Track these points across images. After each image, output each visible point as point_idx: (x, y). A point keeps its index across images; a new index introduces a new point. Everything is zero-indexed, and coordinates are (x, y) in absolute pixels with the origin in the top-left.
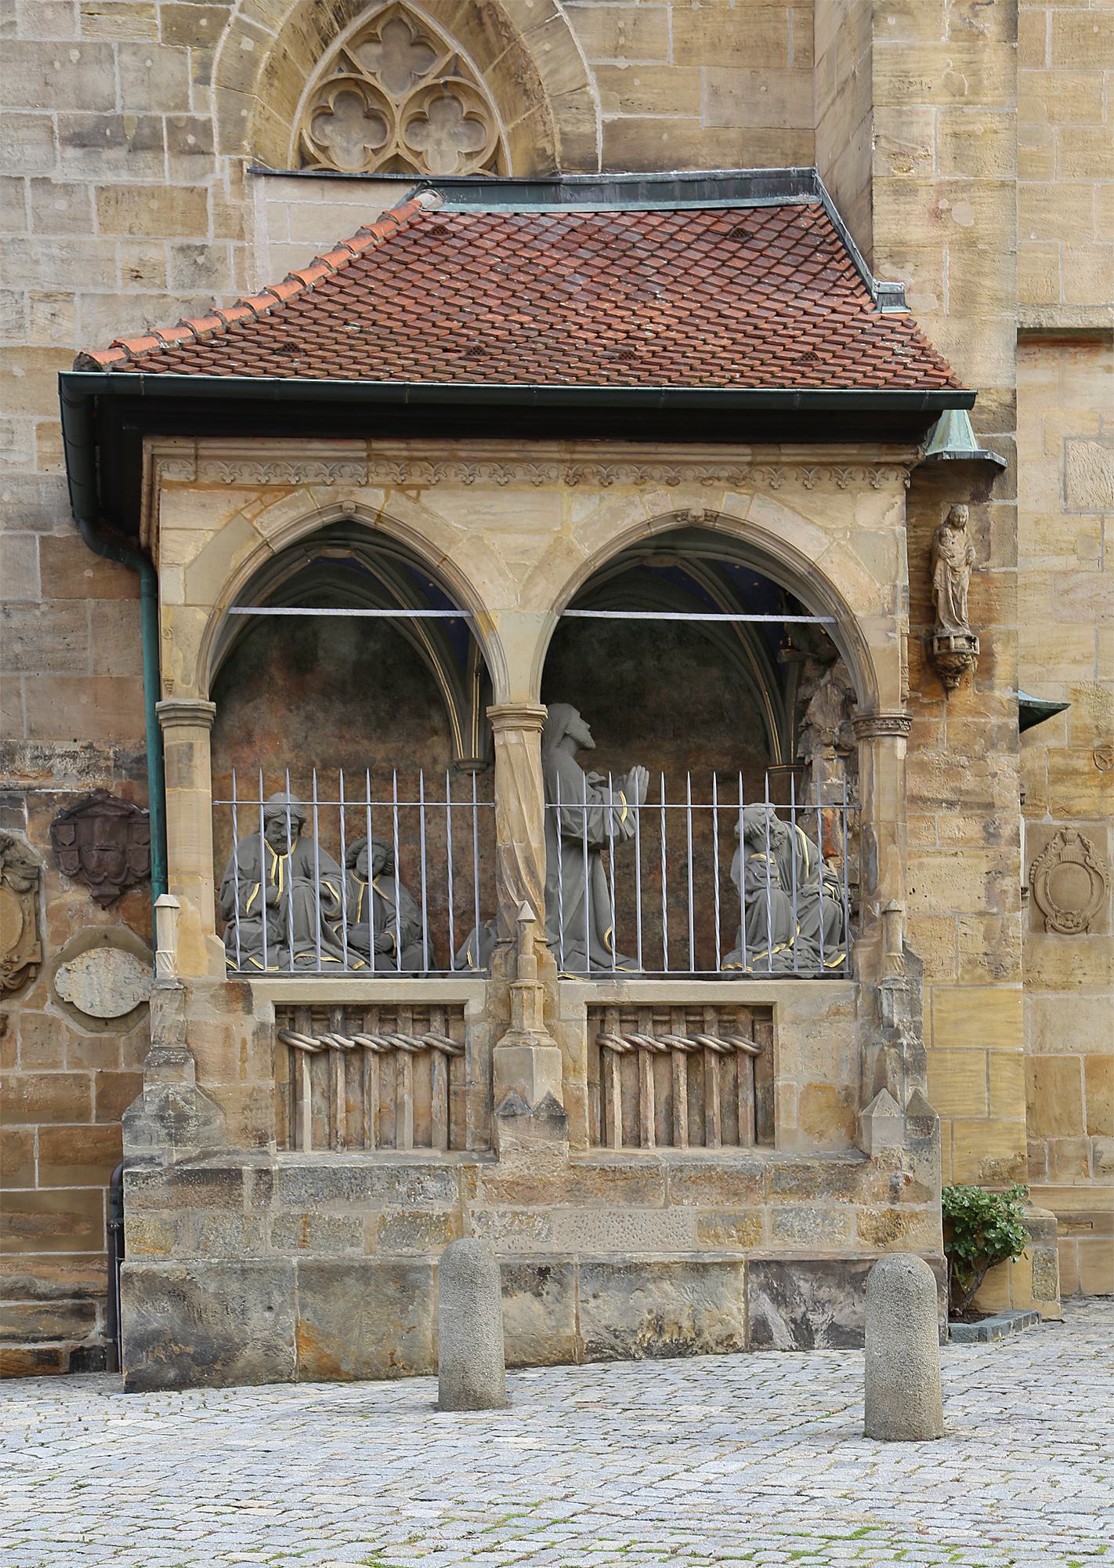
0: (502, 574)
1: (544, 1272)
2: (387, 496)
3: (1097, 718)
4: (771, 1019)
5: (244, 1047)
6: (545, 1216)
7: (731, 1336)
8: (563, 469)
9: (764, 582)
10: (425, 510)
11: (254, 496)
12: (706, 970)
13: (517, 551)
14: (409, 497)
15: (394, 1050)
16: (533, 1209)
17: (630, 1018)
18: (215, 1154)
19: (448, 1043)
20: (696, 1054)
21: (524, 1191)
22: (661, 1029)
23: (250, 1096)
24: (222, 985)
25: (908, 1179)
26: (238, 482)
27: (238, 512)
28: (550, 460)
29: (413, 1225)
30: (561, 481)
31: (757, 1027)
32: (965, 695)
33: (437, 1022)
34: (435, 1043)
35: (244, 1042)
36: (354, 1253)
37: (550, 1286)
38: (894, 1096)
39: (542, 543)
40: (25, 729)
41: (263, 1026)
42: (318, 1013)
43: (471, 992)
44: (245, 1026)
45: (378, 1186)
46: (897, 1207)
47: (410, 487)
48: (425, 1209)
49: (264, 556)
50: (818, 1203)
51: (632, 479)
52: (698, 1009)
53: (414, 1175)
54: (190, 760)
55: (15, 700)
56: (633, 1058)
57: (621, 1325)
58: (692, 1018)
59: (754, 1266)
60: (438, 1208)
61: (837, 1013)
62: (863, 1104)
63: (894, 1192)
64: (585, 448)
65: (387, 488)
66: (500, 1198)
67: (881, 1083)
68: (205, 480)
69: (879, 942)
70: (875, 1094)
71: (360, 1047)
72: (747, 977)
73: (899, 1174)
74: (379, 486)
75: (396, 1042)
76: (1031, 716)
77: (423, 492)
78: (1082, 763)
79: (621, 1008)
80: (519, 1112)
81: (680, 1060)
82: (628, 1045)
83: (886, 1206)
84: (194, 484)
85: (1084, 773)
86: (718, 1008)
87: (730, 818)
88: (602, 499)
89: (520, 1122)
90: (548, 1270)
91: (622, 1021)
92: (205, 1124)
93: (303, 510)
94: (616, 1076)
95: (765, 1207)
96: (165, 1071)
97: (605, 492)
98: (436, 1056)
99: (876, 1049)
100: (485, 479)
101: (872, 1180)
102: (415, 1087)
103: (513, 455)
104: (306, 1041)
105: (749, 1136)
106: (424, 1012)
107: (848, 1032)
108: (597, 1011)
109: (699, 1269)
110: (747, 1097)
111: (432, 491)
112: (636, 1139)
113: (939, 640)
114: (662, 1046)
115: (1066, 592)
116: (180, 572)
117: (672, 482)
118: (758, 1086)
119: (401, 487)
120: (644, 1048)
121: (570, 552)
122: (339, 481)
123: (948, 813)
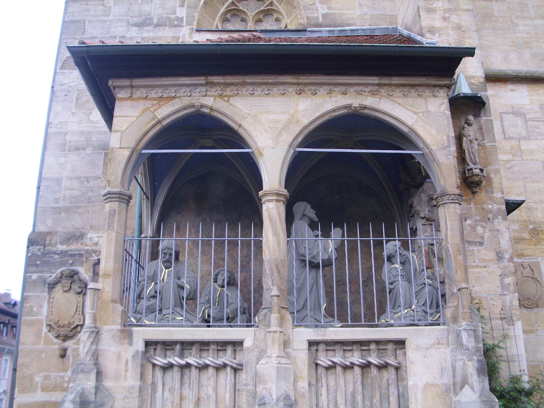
0: (266, 131)
2: (215, 100)
3: (529, 217)
4: (404, 348)
5: (127, 364)
8: (295, 87)
9: (391, 134)
10: (231, 105)
11: (156, 102)
12: (371, 323)
13: (273, 124)
14: (224, 100)
15: (206, 367)
17: (331, 348)
20: (366, 367)
22: (348, 354)
23: (128, 391)
24: (118, 330)
26: (149, 97)
27: (148, 109)
30: (294, 93)
31: (398, 352)
32: (482, 195)
33: (229, 349)
35: (127, 361)
39: (285, 118)
40: (89, 226)
41: (137, 352)
47: (226, 96)
49: (159, 127)
51: (326, 92)
52: (367, 343)
54: (114, 217)
55: (86, 214)
56: (333, 370)
58: (364, 348)
64: (304, 77)
65: (215, 97)
68: (135, 96)
72: (392, 325)
74: (212, 96)
76: (512, 206)
77: (231, 98)
78: (526, 235)
80: (268, 402)
81: (357, 370)
85: (527, 240)
86: (378, 342)
87: (379, 245)
88: (312, 100)
91: (327, 350)
94: (324, 380)
96: (81, 376)
97: (314, 97)
98: (229, 369)
100: (259, 92)
103: (271, 81)
111: (235, 97)
113: (468, 170)
114: (348, 363)
115: (510, 168)
116: (119, 134)
117: (345, 93)
119: (221, 96)
120: (339, 365)
121: (298, 122)
122: (193, 94)
123: (480, 248)
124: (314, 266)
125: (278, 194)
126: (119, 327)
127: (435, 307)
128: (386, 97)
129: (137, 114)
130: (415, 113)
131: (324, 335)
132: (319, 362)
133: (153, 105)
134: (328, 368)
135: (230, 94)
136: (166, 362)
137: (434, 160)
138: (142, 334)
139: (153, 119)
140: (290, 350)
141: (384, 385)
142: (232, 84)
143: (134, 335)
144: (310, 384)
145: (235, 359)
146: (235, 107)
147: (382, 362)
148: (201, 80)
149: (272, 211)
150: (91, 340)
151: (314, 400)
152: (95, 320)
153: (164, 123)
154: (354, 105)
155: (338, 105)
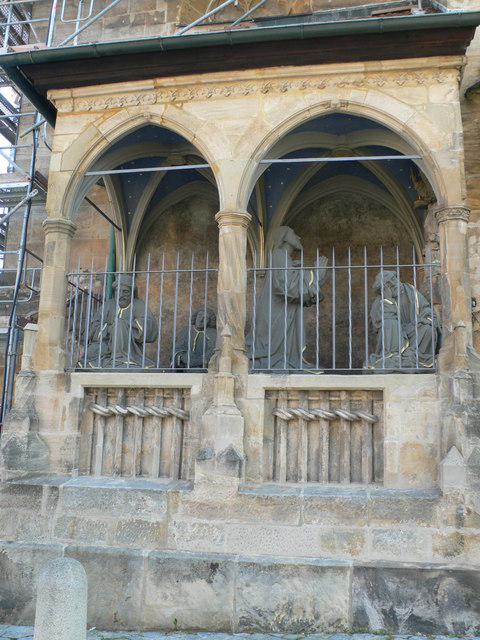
1: (214, 567)
4: (382, 400)
6: (220, 528)
7: (339, 620)
12: (342, 368)
16: (211, 522)
18: (39, 475)
19: (180, 413)
20: (334, 420)
21: (208, 509)
25: (469, 511)
28: (250, 80)
29: (138, 528)
31: (375, 404)
34: (173, 412)
36: (102, 544)
37: (218, 577)
38: (460, 451)
42: (107, 392)
43: (193, 381)
44: (66, 399)
45: (119, 502)
46: (462, 531)
47: (179, 102)
48: (144, 518)
49: (104, 144)
50: (405, 527)
53: (140, 495)
57: (264, 606)
59: (359, 570)
60: (154, 519)
61: (425, 395)
62: (443, 457)
63: (460, 521)
65: (166, 103)
66: (193, 514)
67: (451, 444)
68: (77, 110)
69: (453, 348)
70: (448, 451)
71: (131, 414)
72: (372, 373)
73: (463, 506)
74: (163, 103)
75: (151, 411)
79: (287, 391)
81: (324, 425)
82: (290, 416)
83: (452, 529)
84: (72, 112)
86: (349, 392)
88: (281, 99)
89: (208, 463)
90: (217, 565)
92: (34, 457)
93: (123, 119)
94: (283, 435)
95: (369, 529)
97: (283, 95)
99: (449, 419)
101: (444, 511)
102: (161, 439)
103: (230, 79)
104: (100, 409)
105: (367, 477)
106: (167, 393)
107: (435, 406)
108: (268, 392)
109: (319, 570)
110: (367, 453)
112: (293, 477)
114: (312, 416)
117: (322, 87)
118: (375, 443)
119: (173, 102)
121: (262, 127)
124: (294, 302)
125: (237, 216)
126: (57, 372)
127: (428, 351)
128: (374, 89)
129: (80, 131)
130: (411, 106)
131: (283, 382)
132: (278, 414)
133: (97, 119)
134: (288, 421)
135: (184, 98)
136: (107, 410)
137: (433, 166)
138: (80, 380)
139: (97, 135)
140: (242, 399)
141: (356, 444)
142: (186, 86)
143: (73, 380)
144: (266, 440)
145: (183, 408)
146: (189, 114)
147: (354, 416)
148: (149, 83)
149: (232, 236)
150: (26, 386)
151: (271, 458)
152: (32, 364)
153: (111, 139)
154: (333, 102)
155: (313, 102)
